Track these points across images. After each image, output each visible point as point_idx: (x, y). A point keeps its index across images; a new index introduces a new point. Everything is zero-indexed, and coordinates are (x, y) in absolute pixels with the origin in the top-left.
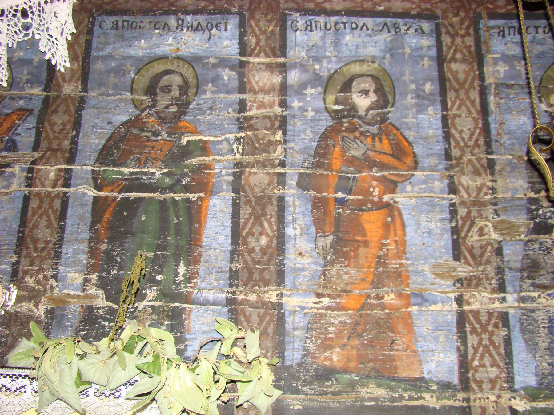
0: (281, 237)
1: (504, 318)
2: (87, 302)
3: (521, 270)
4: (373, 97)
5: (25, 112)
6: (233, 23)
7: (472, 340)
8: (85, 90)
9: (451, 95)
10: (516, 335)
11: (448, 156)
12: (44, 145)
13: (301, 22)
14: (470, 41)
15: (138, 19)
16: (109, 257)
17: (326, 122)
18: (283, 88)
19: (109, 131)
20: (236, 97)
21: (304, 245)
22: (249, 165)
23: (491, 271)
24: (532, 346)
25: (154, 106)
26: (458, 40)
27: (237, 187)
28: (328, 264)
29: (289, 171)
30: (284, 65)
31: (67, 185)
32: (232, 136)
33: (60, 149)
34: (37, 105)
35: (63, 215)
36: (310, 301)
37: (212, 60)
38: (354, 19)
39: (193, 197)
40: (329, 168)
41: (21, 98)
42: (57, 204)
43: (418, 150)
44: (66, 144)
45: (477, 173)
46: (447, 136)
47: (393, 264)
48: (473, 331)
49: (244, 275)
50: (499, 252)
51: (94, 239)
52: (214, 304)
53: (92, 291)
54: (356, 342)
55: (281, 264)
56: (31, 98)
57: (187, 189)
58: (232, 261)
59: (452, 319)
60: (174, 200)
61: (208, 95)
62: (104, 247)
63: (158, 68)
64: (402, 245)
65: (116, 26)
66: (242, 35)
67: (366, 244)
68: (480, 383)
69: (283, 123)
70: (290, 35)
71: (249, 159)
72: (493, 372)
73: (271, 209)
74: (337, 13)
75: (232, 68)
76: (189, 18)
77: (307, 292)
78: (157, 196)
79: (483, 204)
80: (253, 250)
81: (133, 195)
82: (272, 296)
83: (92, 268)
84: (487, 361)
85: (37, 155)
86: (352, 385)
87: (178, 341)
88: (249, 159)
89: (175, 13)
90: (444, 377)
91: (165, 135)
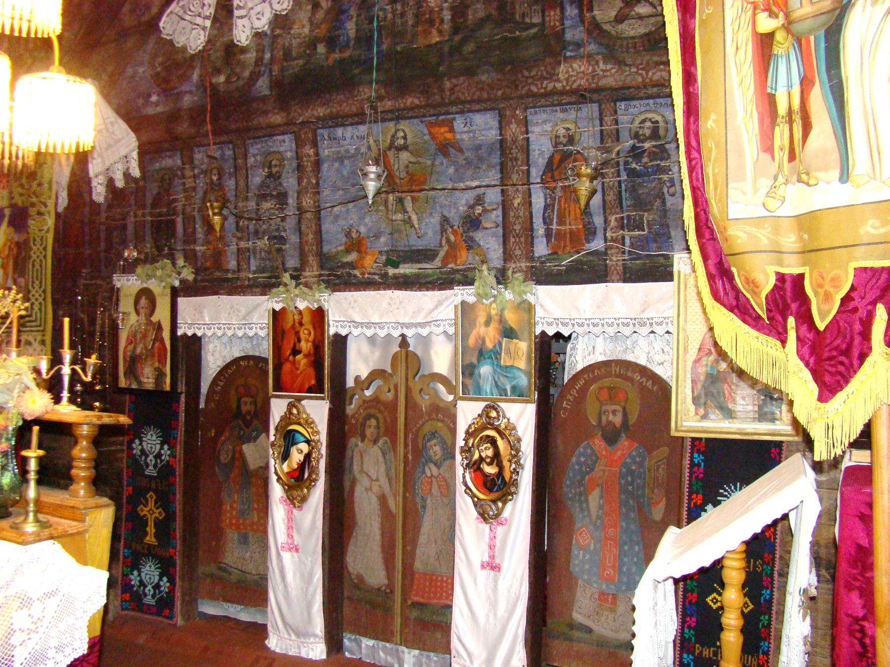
1: (248, 250)
5: (132, 193)
6: (178, 153)
14: (243, 150)
24: (255, 257)
27: (183, 214)
35: (144, 227)
36: (202, 248)
59: (235, 250)
63: (163, 172)
69: (194, 189)
82: (192, 247)
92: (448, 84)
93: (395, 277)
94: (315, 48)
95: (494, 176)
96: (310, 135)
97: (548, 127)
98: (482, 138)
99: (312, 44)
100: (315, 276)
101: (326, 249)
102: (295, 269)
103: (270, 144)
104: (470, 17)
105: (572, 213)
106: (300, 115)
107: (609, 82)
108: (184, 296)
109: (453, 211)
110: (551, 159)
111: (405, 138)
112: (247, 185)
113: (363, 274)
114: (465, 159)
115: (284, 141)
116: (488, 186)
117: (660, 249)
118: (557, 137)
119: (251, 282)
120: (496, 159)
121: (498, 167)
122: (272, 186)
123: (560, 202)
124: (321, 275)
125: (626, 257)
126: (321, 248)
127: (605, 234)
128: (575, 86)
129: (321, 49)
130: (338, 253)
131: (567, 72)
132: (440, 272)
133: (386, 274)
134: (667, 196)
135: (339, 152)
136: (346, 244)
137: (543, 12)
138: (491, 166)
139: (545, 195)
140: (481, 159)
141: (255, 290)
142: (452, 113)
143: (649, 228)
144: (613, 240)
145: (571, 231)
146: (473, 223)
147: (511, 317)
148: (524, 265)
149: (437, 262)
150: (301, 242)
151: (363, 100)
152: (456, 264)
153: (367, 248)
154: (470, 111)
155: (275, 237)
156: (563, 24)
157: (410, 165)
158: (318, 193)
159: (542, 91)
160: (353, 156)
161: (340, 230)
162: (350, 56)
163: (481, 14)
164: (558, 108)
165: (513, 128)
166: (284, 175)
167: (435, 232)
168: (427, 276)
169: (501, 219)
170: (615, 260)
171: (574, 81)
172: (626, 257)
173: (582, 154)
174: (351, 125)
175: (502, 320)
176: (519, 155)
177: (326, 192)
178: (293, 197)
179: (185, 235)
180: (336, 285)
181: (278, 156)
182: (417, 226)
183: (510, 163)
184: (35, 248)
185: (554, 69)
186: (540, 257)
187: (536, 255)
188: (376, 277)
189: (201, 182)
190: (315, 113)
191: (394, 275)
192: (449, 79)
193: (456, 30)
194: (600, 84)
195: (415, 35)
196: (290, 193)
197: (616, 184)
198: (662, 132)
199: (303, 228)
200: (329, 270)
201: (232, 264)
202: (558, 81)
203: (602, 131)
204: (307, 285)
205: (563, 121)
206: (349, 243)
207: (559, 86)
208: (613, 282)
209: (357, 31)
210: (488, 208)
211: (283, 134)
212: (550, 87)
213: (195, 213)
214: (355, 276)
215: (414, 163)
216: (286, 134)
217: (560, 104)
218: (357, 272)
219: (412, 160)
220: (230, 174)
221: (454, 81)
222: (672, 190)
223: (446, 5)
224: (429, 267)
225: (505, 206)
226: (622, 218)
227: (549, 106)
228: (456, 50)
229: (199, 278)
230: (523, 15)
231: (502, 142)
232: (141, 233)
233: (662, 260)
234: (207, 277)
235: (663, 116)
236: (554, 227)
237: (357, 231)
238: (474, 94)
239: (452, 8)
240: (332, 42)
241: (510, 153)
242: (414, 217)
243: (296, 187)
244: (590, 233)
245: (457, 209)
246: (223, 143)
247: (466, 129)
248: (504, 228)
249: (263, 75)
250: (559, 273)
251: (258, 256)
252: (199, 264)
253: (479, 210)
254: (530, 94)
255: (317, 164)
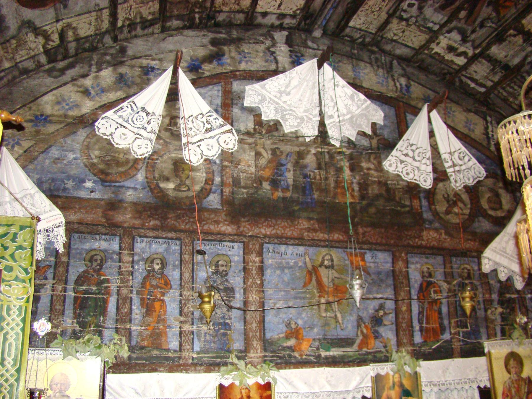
0: (131, 309)
1: (192, 333)
2: (73, 328)
3: (198, 319)
4: (160, 266)
5: (49, 266)
6: (118, 239)
7: (183, 338)
8: (69, 259)
9: (183, 266)
10: (195, 337)
11: (181, 285)
12: (56, 278)
13: (139, 240)
14: (191, 248)
15: (86, 235)
16: (80, 315)
17: (145, 273)
18: (133, 262)
19: (78, 274)
20: (118, 264)
21: (137, 311)
22: (122, 287)
23: (190, 319)
24: (199, 340)
25: (92, 266)
26: (187, 247)
27: (118, 294)
28: (144, 317)
29: (134, 289)
30: (133, 254)
31: (65, 291)
32: (116, 277)
33: (62, 280)
34: (53, 264)
35: (64, 301)
36: (139, 328)
37: (111, 251)
38: (156, 240)
39: (105, 297)
40: (146, 289)
41: (47, 261)
42: (62, 298)
43: (172, 283)
44: (64, 278)
45: (188, 290)
46: (181, 279)
47: (162, 317)
48: (184, 336)
49: (120, 320)
50: (193, 314)
51: (75, 309)
52: (111, 328)
53: (75, 325)
54: (151, 339)
55: (131, 317)
56: (50, 261)
57: (103, 294)
58: (116, 316)
59: (178, 332)
60: (99, 298)
61: (109, 263)
62: (78, 311)
63: (93, 253)
64: (165, 312)
65: (79, 237)
66: (120, 243)
67: (155, 311)
68: (184, 350)
69: (132, 273)
70: (135, 244)
71: (122, 285)
72: (188, 347)
73: (128, 301)
74: (151, 237)
75: (117, 255)
76: (103, 236)
77: (138, 325)
78: (94, 296)
79: (189, 300)
80: (122, 313)
81: (86, 296)
82: (128, 327)
83: (74, 318)
84: (187, 344)
85: (54, 282)
86: (150, 351)
87: (101, 339)
88: (122, 285)
89: (99, 234)
90: (174, 348)
91: (96, 276)
92: (361, 230)
93: (326, 358)
94: (261, 184)
95: (389, 293)
96: (257, 247)
97: (418, 266)
98: (382, 267)
99: (259, 180)
100: (260, 357)
101: (268, 335)
102: (241, 351)
103: (220, 248)
104: (370, 192)
105: (433, 317)
106: (250, 231)
107: (446, 245)
108: (113, 372)
109: (365, 312)
110: (421, 285)
111: (332, 260)
112: (193, 277)
113: (301, 355)
114: (372, 280)
115: (233, 248)
116: (387, 299)
117: (476, 339)
118: (423, 272)
119: (195, 361)
120: (390, 281)
121: (392, 287)
122: (219, 281)
123: (427, 311)
124: (265, 356)
125: (461, 343)
126: (264, 334)
127: (450, 330)
128: (432, 244)
129: (266, 186)
130: (279, 339)
131: (427, 236)
132: (359, 354)
133: (319, 356)
134: (477, 310)
135: (281, 263)
136: (286, 332)
137: (411, 199)
138: (387, 286)
139: (419, 306)
140: (382, 281)
141: (198, 368)
142: (364, 249)
143: (471, 327)
144: (455, 334)
145: (433, 328)
146: (377, 321)
147: (407, 384)
148: (410, 348)
149: (355, 347)
150: (245, 329)
151: (302, 229)
152: (368, 349)
153: (303, 336)
154: (375, 250)
155: (220, 324)
156: (421, 209)
157: (336, 279)
158: (263, 291)
159: (415, 244)
160: (291, 267)
161: (281, 321)
162: (291, 197)
163: (376, 191)
164: (424, 256)
165: (400, 264)
166: (231, 273)
167: (353, 327)
168: (350, 357)
169: (394, 319)
170: (457, 345)
171: (431, 242)
172: (461, 343)
173: (437, 284)
174: (293, 245)
175: (401, 385)
176: (404, 281)
177: (269, 292)
178: (240, 293)
179: (117, 314)
180: (280, 364)
181: (227, 259)
182: (341, 322)
183: (399, 285)
184: (9, 319)
185: (420, 233)
186: (418, 344)
187: (416, 342)
188: (312, 358)
189: (141, 269)
190: (263, 231)
191: (326, 356)
192: (361, 227)
193: (363, 197)
194: (443, 245)
195: (335, 195)
196: (237, 289)
197: (454, 302)
198: (472, 276)
199: (248, 317)
200: (272, 352)
201: (174, 344)
202: (423, 240)
203: (445, 272)
204: (251, 363)
205: (426, 263)
206: (288, 332)
207: (423, 243)
208: (455, 357)
209: (294, 181)
210: (387, 312)
211: (233, 241)
212: (419, 243)
213: (134, 296)
214: (295, 357)
215: (338, 278)
216: (236, 242)
217: (424, 254)
218: (296, 354)
219: (337, 275)
220: (174, 266)
221: (365, 229)
222: (479, 307)
223: (355, 181)
224: (351, 351)
225: (397, 311)
226: (457, 321)
227: (419, 254)
228: (364, 209)
229: (134, 356)
230: (400, 199)
231: (393, 271)
232: (58, 307)
233: (478, 345)
234: (144, 356)
235: (472, 267)
236: (424, 325)
237: (296, 323)
238: (377, 239)
239: (359, 184)
240: (275, 183)
241: (399, 279)
242: (339, 315)
243: (242, 284)
244: (443, 330)
245: (368, 311)
246: (172, 239)
247: (372, 260)
248: (397, 325)
249: (214, 193)
250: (429, 353)
251: (202, 339)
252: (134, 343)
253: (381, 313)
254: (409, 245)
255: (261, 270)
